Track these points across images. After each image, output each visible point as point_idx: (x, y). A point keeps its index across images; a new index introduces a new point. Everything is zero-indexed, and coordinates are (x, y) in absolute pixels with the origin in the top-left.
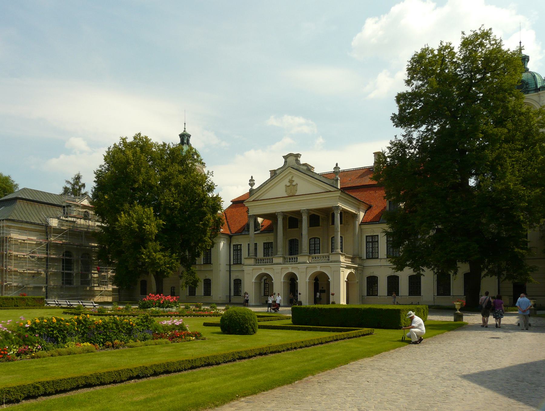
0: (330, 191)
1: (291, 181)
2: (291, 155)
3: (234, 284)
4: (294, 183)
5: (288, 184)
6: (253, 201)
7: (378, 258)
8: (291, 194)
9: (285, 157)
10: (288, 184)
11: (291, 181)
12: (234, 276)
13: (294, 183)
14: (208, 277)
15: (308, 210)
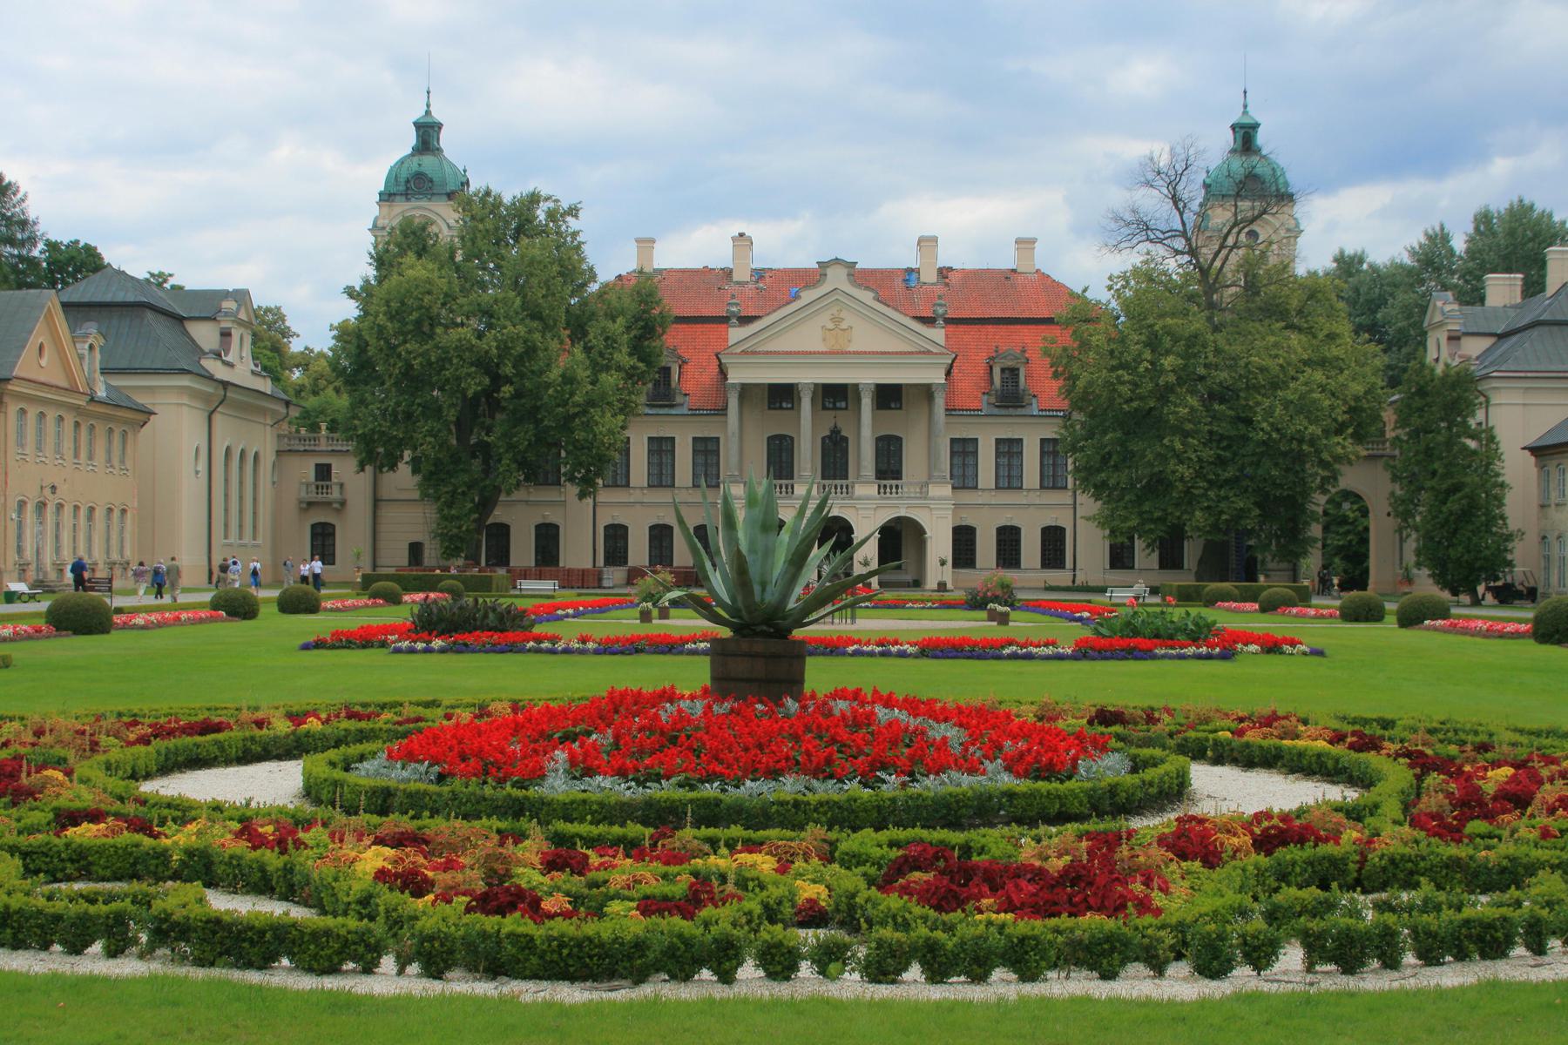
0: (929, 352)
1: (837, 320)
2: (837, 261)
3: (606, 536)
4: (844, 325)
5: (831, 326)
6: (744, 352)
7: (976, 488)
8: (837, 348)
9: (823, 265)
10: (831, 326)
11: (837, 320)
12: (605, 519)
13: (844, 325)
14: (552, 516)
15: (878, 386)
